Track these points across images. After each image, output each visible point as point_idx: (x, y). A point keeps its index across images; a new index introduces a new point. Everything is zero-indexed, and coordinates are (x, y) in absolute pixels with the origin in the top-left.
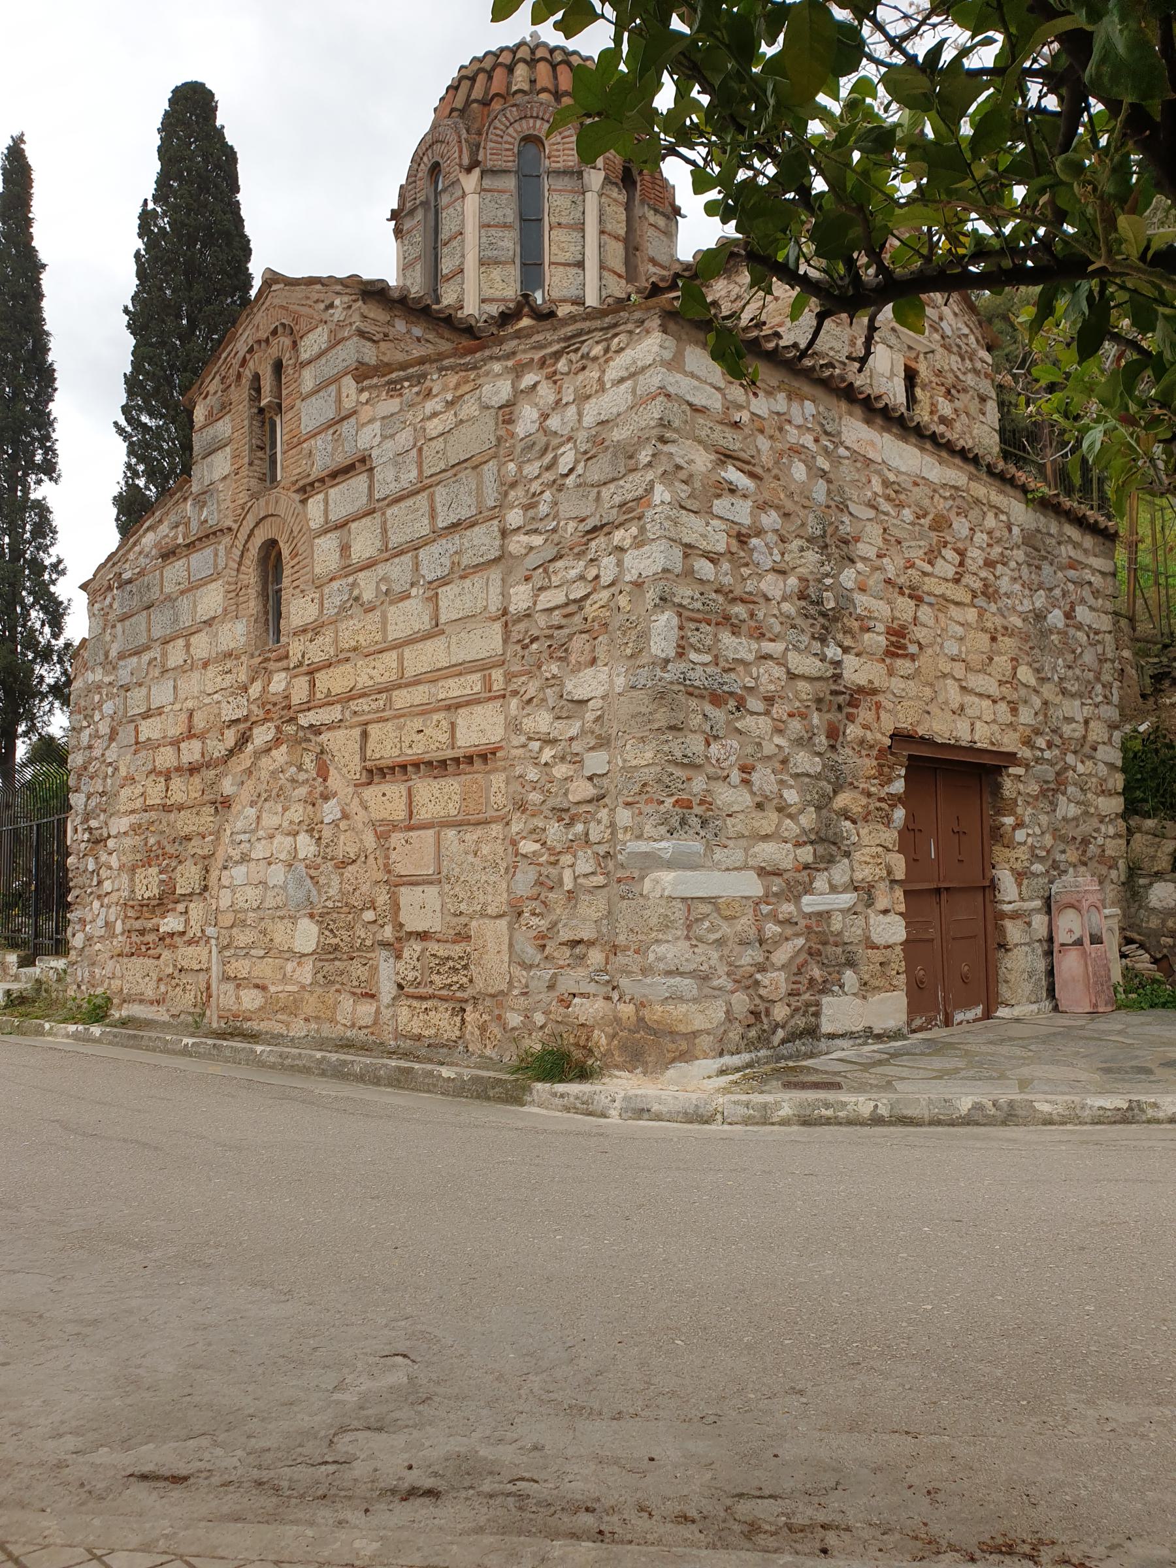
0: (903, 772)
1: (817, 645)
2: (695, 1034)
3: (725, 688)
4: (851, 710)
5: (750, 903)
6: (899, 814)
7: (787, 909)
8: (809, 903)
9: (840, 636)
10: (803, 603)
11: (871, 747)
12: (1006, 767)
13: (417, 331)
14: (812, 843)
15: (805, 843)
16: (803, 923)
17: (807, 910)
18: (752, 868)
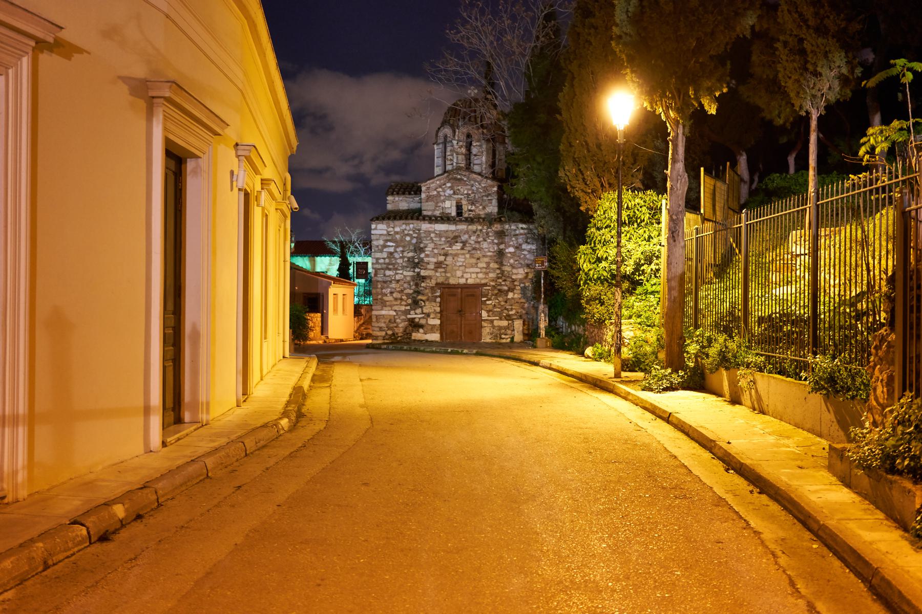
6: (438, 300)
8: (409, 316)
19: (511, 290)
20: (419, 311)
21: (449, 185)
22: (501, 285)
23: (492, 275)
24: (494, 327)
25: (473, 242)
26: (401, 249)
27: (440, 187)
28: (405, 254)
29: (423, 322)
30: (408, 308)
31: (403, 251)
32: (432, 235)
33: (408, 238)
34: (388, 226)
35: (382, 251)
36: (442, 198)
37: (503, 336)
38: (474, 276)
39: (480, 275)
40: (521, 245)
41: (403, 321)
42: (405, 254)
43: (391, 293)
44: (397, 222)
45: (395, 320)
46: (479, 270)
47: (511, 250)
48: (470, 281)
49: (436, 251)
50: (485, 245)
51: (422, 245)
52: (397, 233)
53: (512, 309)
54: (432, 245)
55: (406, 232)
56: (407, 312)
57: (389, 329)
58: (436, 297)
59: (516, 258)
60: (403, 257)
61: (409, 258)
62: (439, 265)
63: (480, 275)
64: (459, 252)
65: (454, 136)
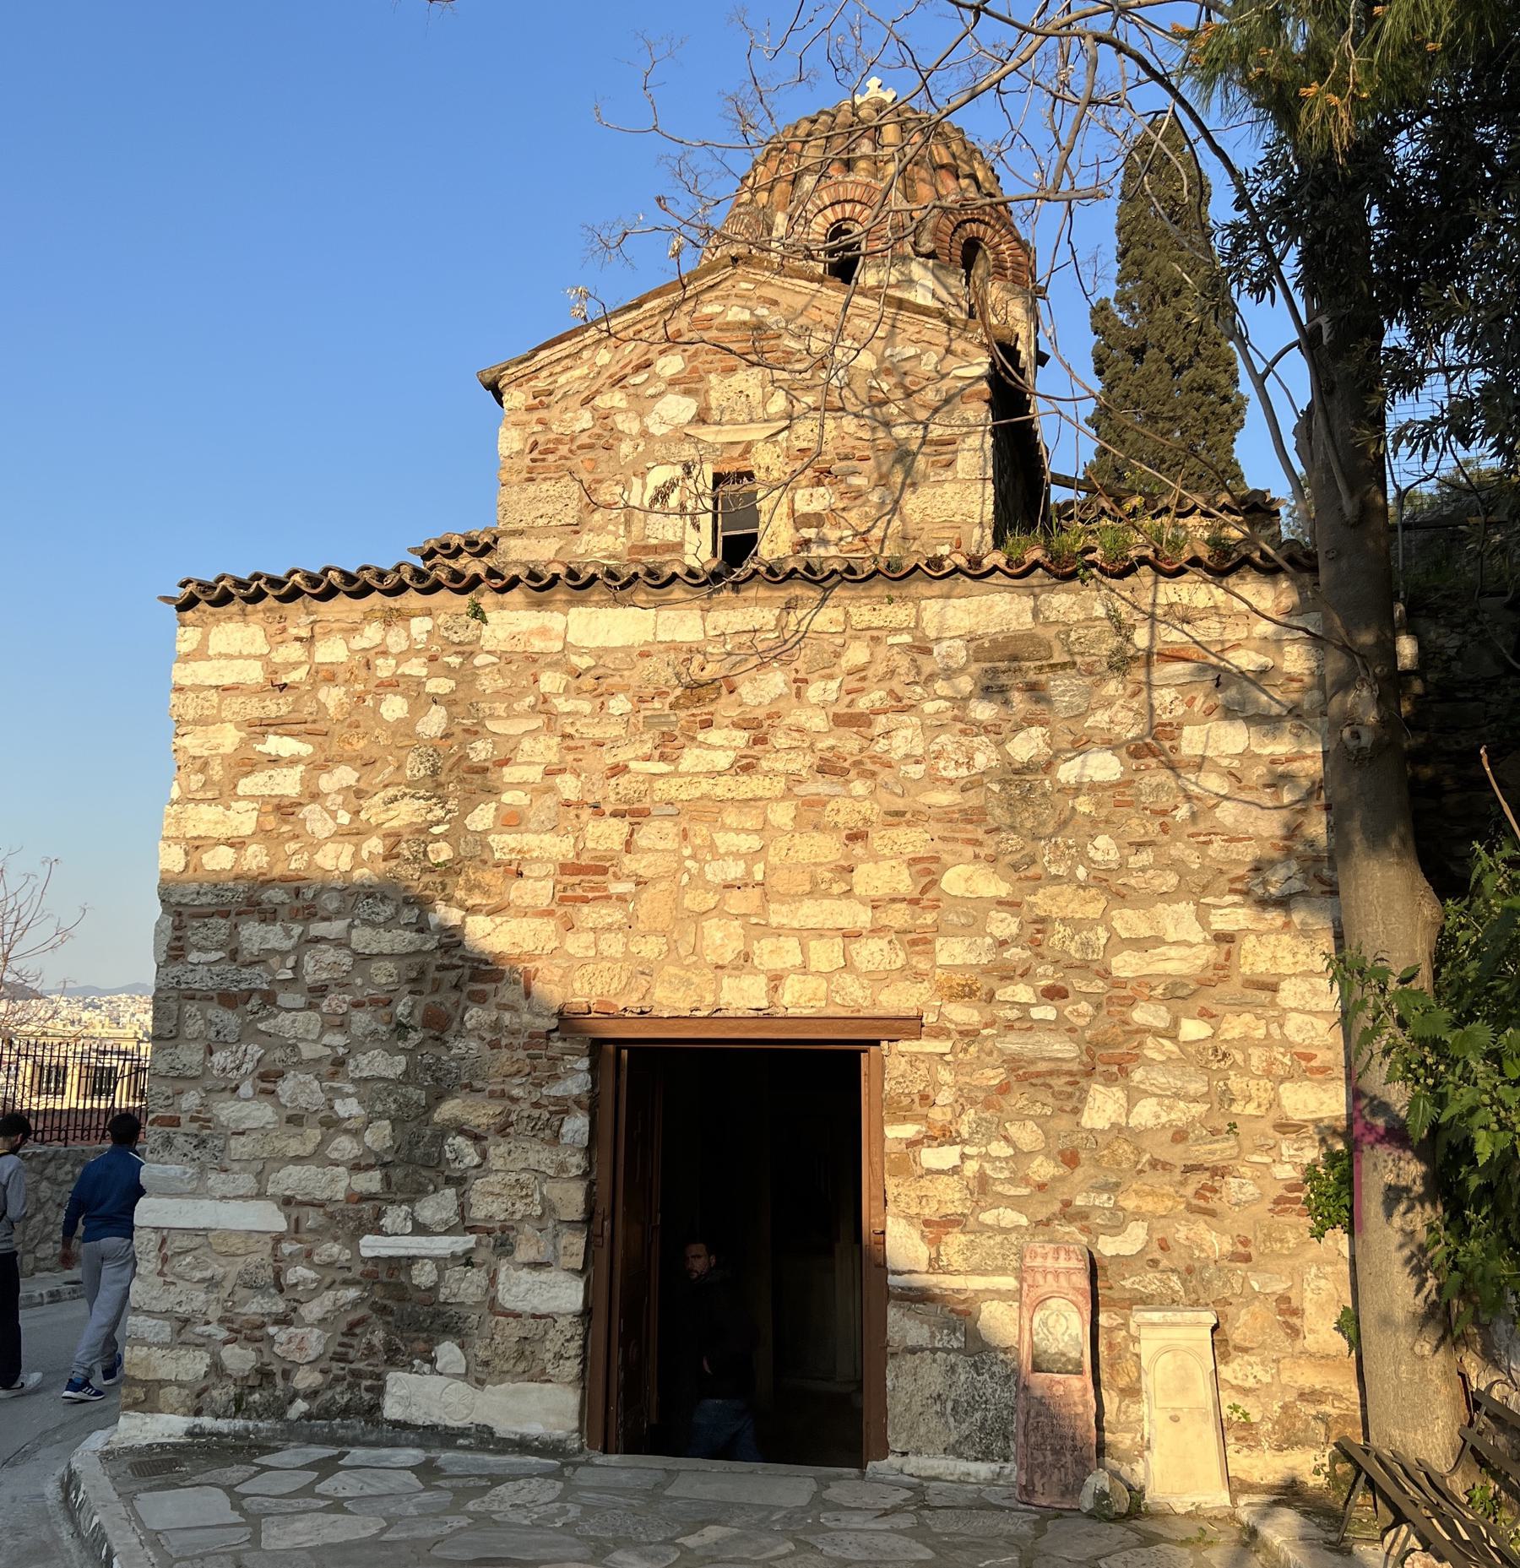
0: (584, 1063)
2: (161, 1383)
3: (243, 986)
5: (267, 1238)
6: (577, 1126)
7: (332, 1250)
8: (372, 1246)
9: (460, 894)
11: (514, 1033)
14: (385, 1165)
15: (369, 1167)
16: (359, 1268)
18: (273, 1197)
19: (1108, 1059)
20: (437, 1207)
22: (1024, 1023)
23: (953, 952)
25: (819, 722)
26: (345, 775)
27: (618, 382)
28: (373, 810)
29: (465, 1287)
30: (371, 1182)
32: (550, 681)
33: (394, 707)
34: (277, 638)
35: (224, 795)
36: (625, 448)
38: (826, 955)
39: (873, 953)
40: (1171, 730)
43: (269, 1078)
46: (865, 918)
49: (568, 786)
50: (905, 739)
51: (481, 751)
53: (1117, 1227)
54: (546, 749)
55: (385, 668)
56: (362, 1216)
57: (250, 1333)
58: (562, 1108)
59: (1137, 827)
60: (355, 834)
61: (395, 837)
64: (722, 788)
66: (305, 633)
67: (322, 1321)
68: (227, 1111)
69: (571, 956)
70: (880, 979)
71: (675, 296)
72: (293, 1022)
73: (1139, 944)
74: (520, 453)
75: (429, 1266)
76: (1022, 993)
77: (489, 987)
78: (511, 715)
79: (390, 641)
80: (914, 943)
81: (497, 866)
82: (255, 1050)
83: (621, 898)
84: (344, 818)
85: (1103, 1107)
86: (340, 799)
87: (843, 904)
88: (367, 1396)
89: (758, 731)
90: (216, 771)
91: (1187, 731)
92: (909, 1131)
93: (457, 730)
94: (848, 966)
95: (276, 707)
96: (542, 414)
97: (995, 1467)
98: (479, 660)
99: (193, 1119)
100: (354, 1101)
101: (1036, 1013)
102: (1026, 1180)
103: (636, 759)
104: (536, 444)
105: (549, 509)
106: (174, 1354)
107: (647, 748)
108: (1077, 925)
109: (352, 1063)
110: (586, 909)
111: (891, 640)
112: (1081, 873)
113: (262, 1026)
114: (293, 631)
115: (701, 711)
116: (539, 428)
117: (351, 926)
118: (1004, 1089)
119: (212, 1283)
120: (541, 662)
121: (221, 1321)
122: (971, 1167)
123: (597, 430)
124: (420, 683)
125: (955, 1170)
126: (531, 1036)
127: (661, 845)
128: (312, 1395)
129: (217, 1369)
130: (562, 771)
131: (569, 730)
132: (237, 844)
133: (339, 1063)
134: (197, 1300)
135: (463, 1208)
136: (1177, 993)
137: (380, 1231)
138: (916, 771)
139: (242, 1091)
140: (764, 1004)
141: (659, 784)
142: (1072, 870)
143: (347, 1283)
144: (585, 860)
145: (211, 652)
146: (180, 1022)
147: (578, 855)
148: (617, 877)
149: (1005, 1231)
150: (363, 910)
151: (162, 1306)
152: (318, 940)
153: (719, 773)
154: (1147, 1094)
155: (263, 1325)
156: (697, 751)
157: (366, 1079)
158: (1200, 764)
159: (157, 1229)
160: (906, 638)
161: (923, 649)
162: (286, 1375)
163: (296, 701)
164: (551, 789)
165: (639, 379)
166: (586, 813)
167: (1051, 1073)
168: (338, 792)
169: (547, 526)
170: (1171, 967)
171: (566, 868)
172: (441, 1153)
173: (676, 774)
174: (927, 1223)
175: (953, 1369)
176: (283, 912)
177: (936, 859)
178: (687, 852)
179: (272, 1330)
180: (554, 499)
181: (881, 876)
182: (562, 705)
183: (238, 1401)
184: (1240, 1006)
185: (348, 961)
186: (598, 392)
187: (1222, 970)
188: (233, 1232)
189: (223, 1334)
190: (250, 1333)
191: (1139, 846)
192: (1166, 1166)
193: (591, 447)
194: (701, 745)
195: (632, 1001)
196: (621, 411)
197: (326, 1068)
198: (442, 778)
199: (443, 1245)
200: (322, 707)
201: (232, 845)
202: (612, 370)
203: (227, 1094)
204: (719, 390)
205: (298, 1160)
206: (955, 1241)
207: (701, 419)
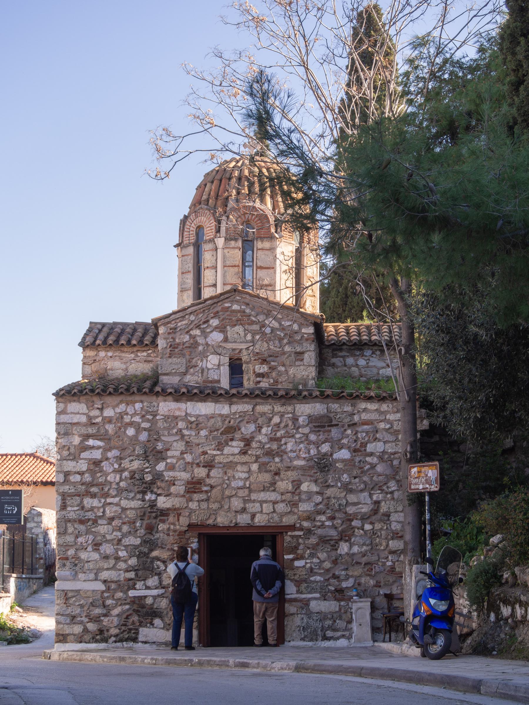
0: (196, 540)
1: (139, 496)
2: (68, 635)
4: (162, 518)
7: (119, 595)
8: (132, 593)
9: (155, 490)
10: (133, 481)
12: (286, 532)
13: (110, 354)
14: (135, 570)
15: (131, 571)
16: (128, 601)
17: (130, 595)
18: (100, 580)
19: (345, 536)
20: (152, 581)
21: (215, 322)
22: (323, 526)
23: (305, 507)
24: (309, 614)
25: (264, 440)
27: (198, 327)
28: (126, 463)
30: (132, 575)
31: (120, 459)
32: (181, 425)
33: (131, 432)
34: (90, 407)
35: (75, 457)
36: (200, 348)
37: (329, 634)
38: (267, 508)
39: (281, 507)
41: (120, 602)
42: (126, 463)
43: (97, 546)
44: (109, 400)
45: (104, 599)
46: (279, 498)
47: (344, 454)
48: (260, 520)
52: (109, 420)
54: (180, 446)
55: (127, 419)
57: (96, 620)
59: (355, 473)
60: (121, 471)
62: (194, 486)
63: (281, 507)
65: (218, 231)
66: (100, 407)
67: (118, 615)
68: (83, 555)
69: (191, 509)
70: (282, 515)
71: (215, 300)
72: (103, 528)
73: (355, 504)
74: (166, 347)
75: (151, 598)
76: (323, 518)
77: (166, 518)
78: (169, 435)
79: (128, 410)
80: (293, 504)
81: (167, 481)
82: (91, 537)
83: (206, 492)
84: (116, 466)
85: (344, 548)
86: (115, 460)
87: (273, 494)
88: (134, 635)
89: (248, 442)
90: (72, 450)
91: (368, 445)
92: (291, 557)
93: (152, 439)
94: (274, 511)
95: (91, 430)
96: (172, 335)
97: (314, 643)
98: (158, 417)
99: (72, 558)
100: (125, 552)
101: (327, 523)
102: (323, 569)
103: (210, 450)
104: (171, 346)
105: (176, 367)
106: (71, 626)
107: (213, 446)
108: (338, 499)
109: (123, 540)
110: (195, 495)
111: (286, 416)
112: (339, 484)
113: (93, 530)
114: (96, 406)
115: (230, 436)
116: (171, 340)
117: (121, 499)
118: (317, 544)
119: (82, 606)
120: (179, 419)
121: (86, 616)
122: (308, 565)
123: (192, 341)
124: (139, 424)
125: (304, 566)
126: (180, 532)
127: (218, 476)
128: (116, 636)
129: (86, 630)
130: (186, 453)
131: (188, 440)
132: (81, 473)
133: (120, 540)
134: (78, 611)
135: (161, 582)
136: (364, 518)
137: (135, 589)
138: (293, 455)
139: (88, 549)
140: (250, 522)
141: (217, 457)
142: (337, 483)
143: (125, 604)
144: (194, 480)
145: (68, 412)
146: (66, 529)
147: (192, 479)
148: (205, 485)
149: (317, 582)
150: (125, 494)
151: (67, 613)
152: (110, 504)
153: (236, 455)
154: (355, 545)
155: (100, 617)
156: (229, 448)
157: (128, 545)
158: (371, 454)
159: (63, 591)
160: (290, 415)
161: (295, 419)
162: (108, 631)
163: (99, 428)
164: (184, 459)
165: (205, 326)
166: (195, 466)
167: (330, 540)
168: (114, 458)
169: (175, 373)
170: (363, 510)
171: (188, 483)
172: (153, 566)
173: (222, 454)
174: (296, 581)
175: (303, 619)
176: (99, 495)
177: (299, 480)
178: (226, 478)
179: (102, 618)
180: (177, 363)
181: (284, 485)
182: (186, 432)
183: (93, 638)
184: (380, 521)
185: (120, 510)
186: (191, 329)
187: (375, 511)
188: (88, 591)
189: (87, 620)
190: (96, 620)
191: (355, 478)
192: (360, 563)
193: (190, 347)
194: (230, 446)
195: (210, 522)
196: (199, 336)
197: (115, 542)
198: (148, 454)
199: (155, 592)
200: (107, 431)
201: (80, 474)
202: (196, 322)
203: (83, 550)
204: (231, 332)
205: (108, 569)
206: (304, 585)
207: (226, 340)
